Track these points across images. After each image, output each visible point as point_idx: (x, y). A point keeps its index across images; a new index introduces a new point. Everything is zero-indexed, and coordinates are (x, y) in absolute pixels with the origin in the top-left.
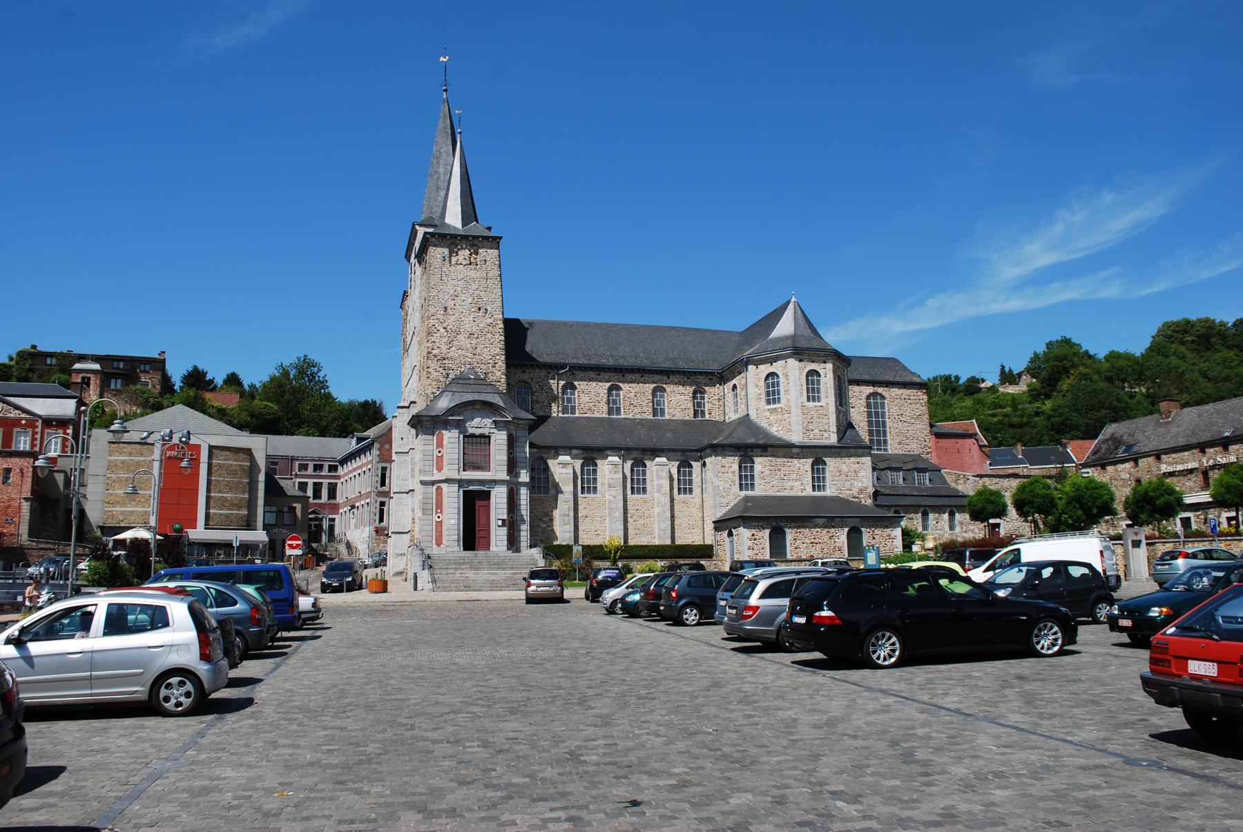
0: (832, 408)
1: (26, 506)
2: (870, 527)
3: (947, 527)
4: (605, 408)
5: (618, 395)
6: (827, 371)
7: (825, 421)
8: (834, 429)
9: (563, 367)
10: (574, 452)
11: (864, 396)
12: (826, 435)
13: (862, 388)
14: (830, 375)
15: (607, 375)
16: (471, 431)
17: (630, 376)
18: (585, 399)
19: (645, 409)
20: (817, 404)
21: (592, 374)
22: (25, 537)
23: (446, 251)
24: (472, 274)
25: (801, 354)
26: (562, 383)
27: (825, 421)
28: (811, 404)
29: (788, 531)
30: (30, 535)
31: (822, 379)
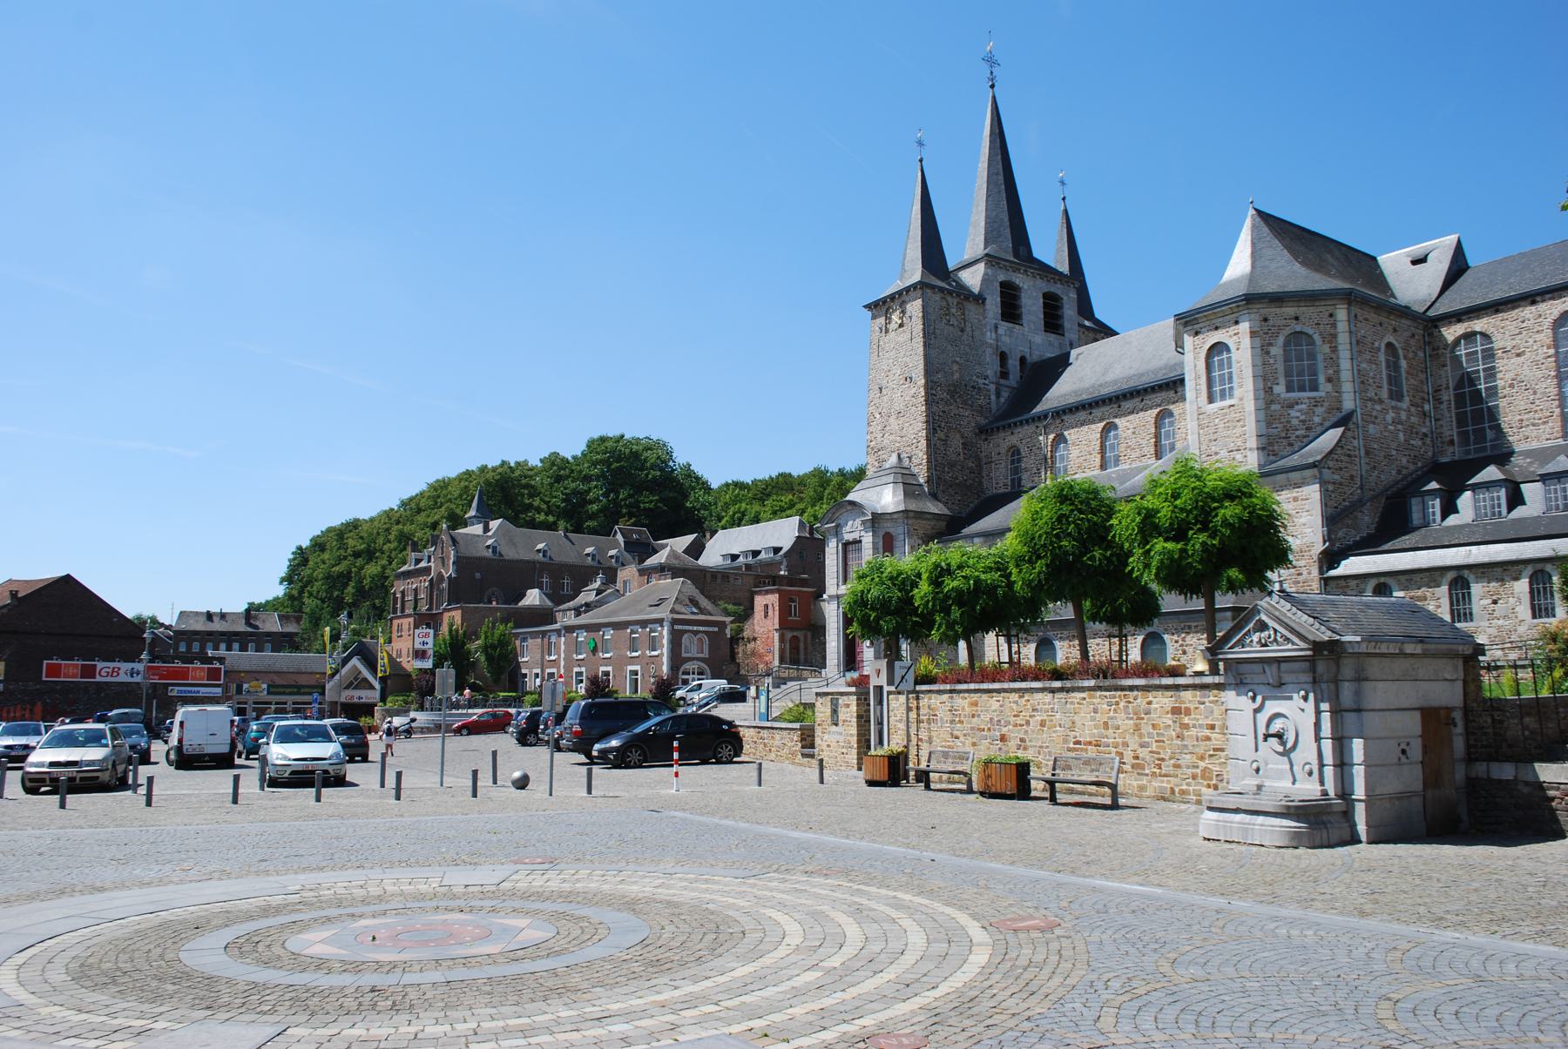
0: (1250, 405)
1: (777, 635)
2: (1177, 631)
3: (1524, 611)
4: (1098, 460)
5: (1116, 437)
6: (1239, 339)
7: (1238, 431)
8: (1253, 442)
9: (1046, 417)
10: (976, 540)
11: (1547, 323)
12: (1239, 457)
13: (1542, 307)
14: (1246, 342)
15: (1097, 412)
16: (848, 537)
17: (1127, 405)
18: (1074, 452)
19: (1145, 450)
20: (1228, 402)
21: (1082, 415)
22: (776, 663)
23: (882, 320)
24: (900, 339)
25: (1196, 322)
26: (1051, 437)
27: (1238, 431)
28: (1218, 404)
29: (1057, 644)
30: (782, 660)
31: (1235, 355)
